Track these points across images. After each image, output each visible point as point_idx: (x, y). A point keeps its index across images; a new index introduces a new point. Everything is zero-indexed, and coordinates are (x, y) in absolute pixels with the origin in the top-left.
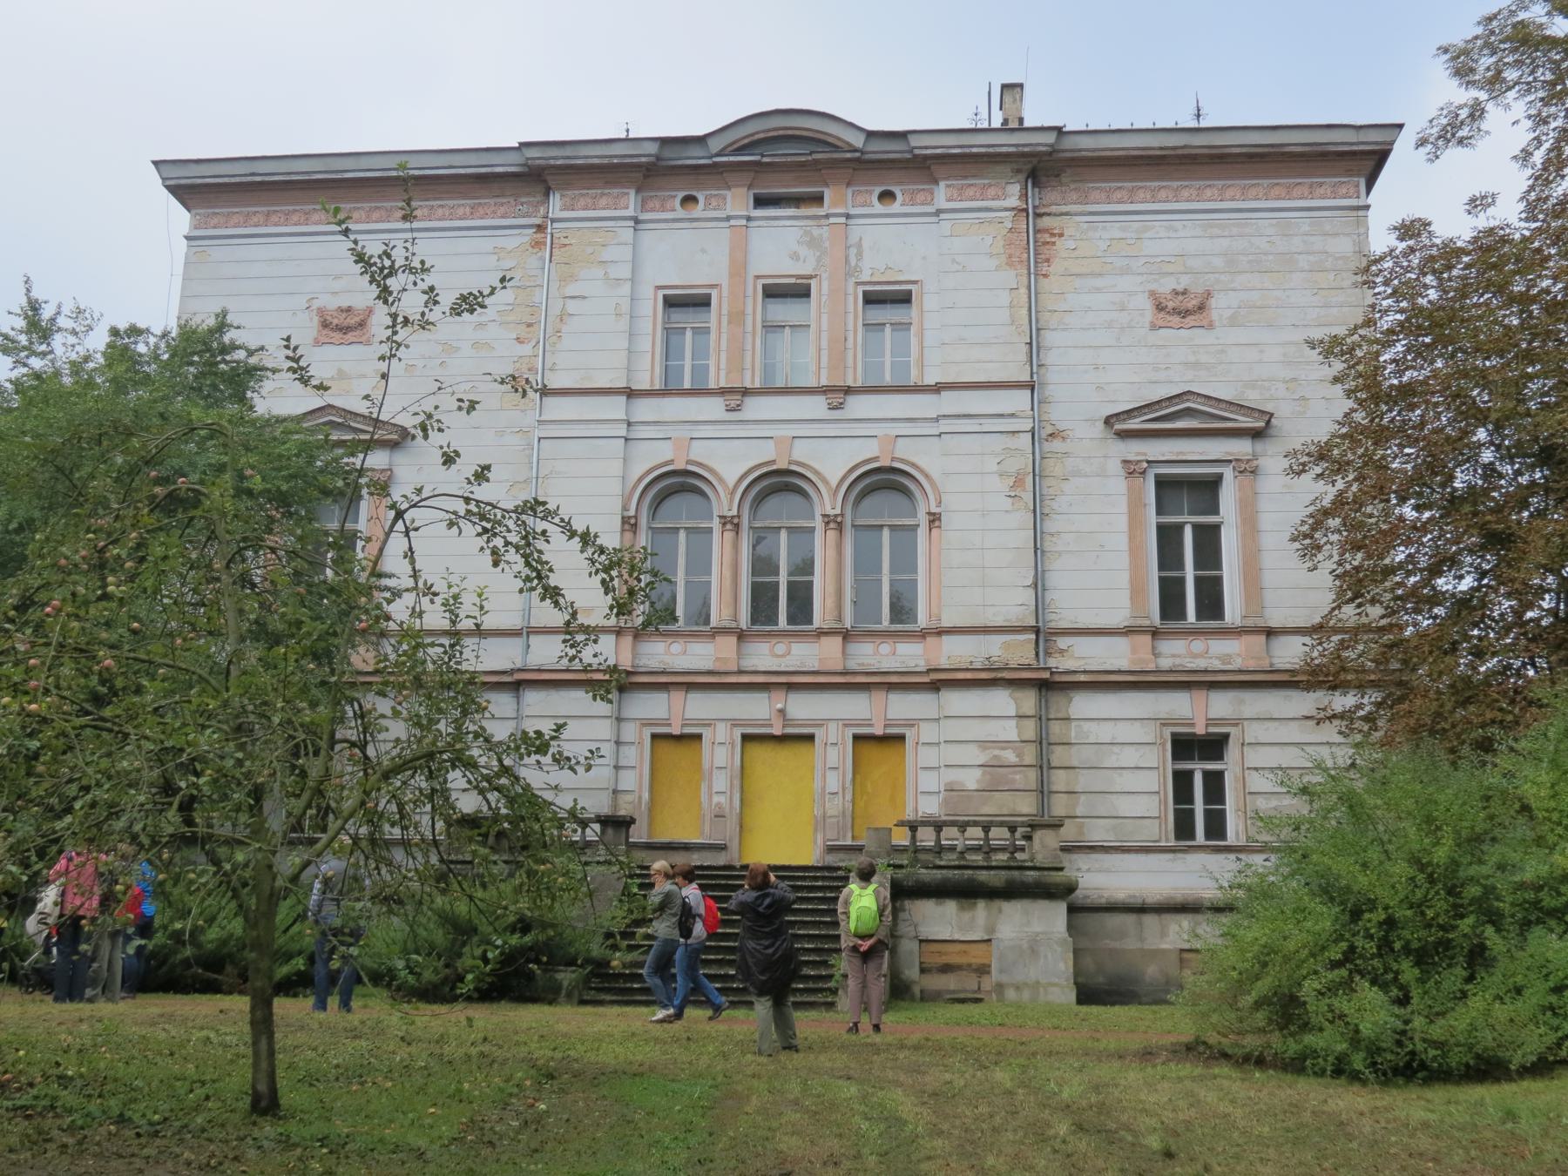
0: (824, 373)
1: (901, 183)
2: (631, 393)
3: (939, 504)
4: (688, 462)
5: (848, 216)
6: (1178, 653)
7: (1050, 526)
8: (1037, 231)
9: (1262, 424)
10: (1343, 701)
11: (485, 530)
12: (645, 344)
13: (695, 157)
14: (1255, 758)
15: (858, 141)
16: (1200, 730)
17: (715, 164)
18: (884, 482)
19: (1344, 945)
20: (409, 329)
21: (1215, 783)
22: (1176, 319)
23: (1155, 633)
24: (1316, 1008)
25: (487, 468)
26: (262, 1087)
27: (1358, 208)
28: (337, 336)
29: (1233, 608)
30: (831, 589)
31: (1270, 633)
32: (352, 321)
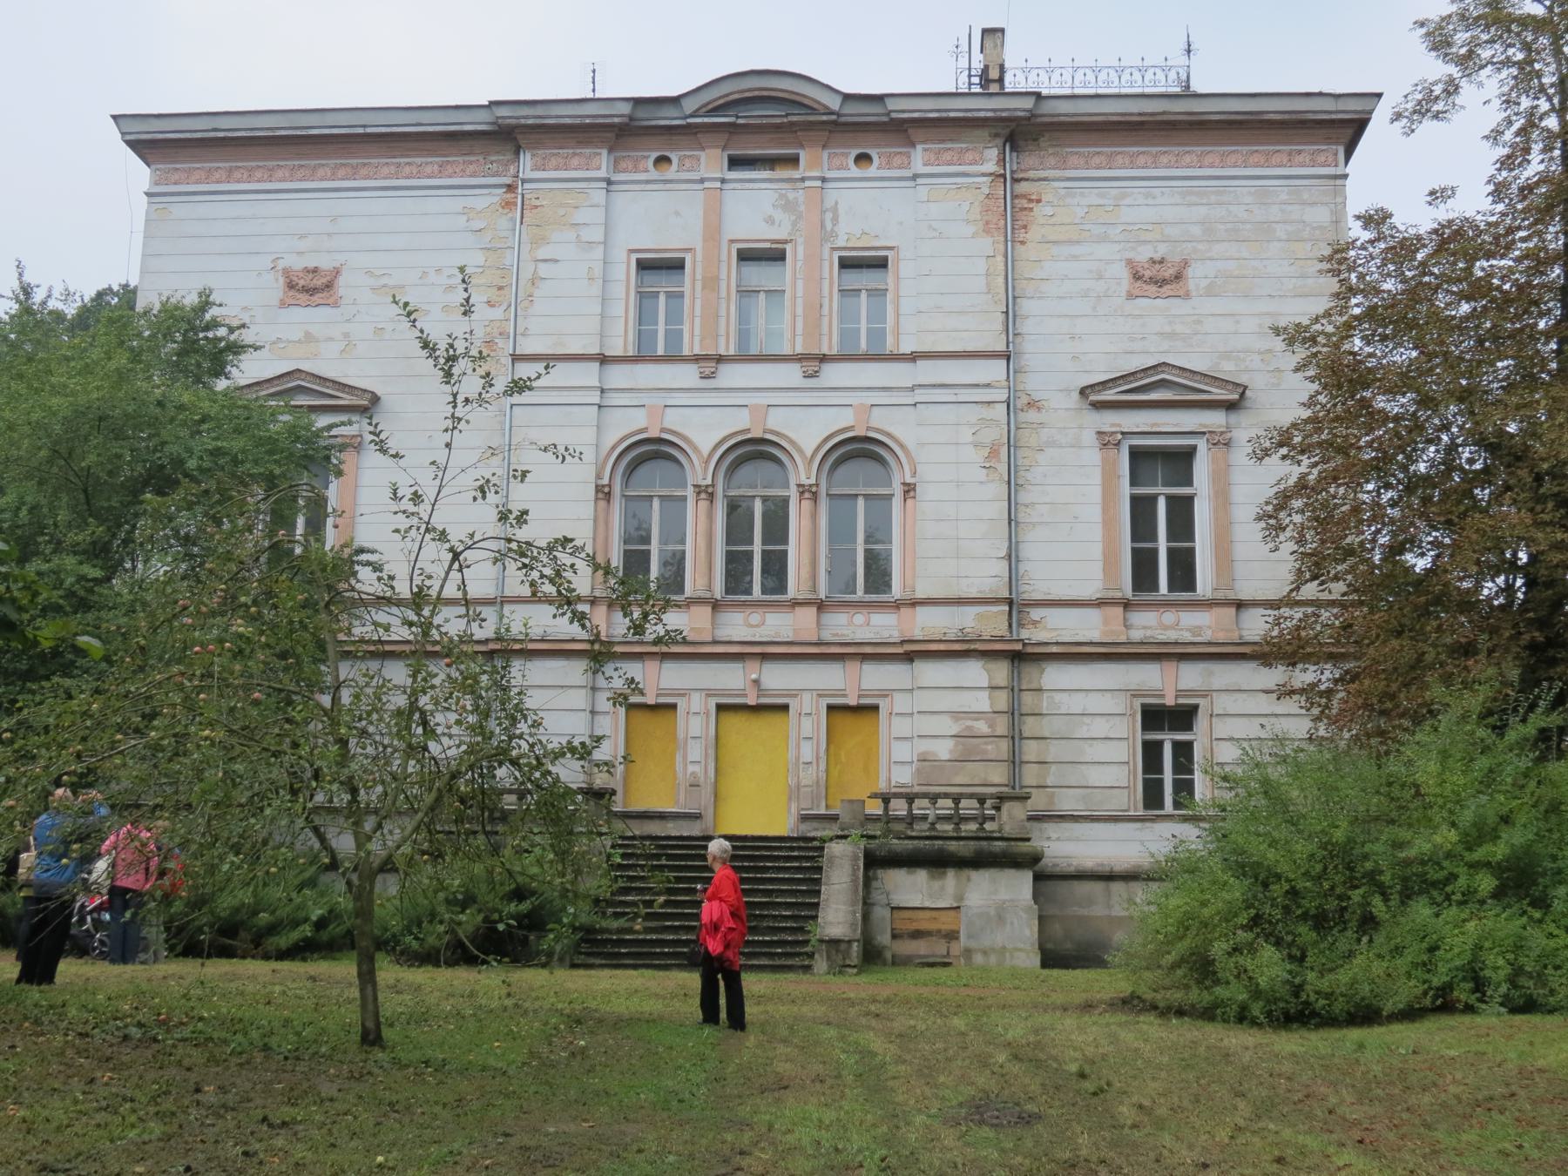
0: (799, 340)
1: (878, 146)
3: (914, 474)
4: (663, 430)
5: (824, 180)
6: (1149, 625)
7: (1024, 497)
8: (1014, 197)
9: (1236, 397)
10: (1305, 676)
11: (525, 566)
12: (618, 309)
13: (668, 117)
15: (834, 103)
16: (1170, 701)
17: (689, 126)
18: (859, 451)
19: (1253, 912)
20: (469, 407)
21: (1184, 751)
22: (1153, 288)
23: (1127, 605)
24: (1225, 966)
25: (526, 512)
26: (370, 1025)
27: (1336, 177)
28: (304, 297)
29: (1205, 579)
30: (806, 560)
31: (1240, 605)
32: (318, 282)
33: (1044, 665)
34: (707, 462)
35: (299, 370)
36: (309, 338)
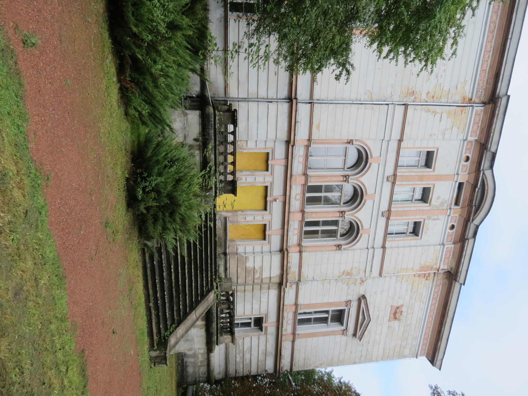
1: (456, 232)
2: (400, 141)
3: (344, 249)
6: (288, 316)
13: (485, 164)
14: (255, 340)
15: (476, 222)
33: (277, 290)
34: (357, 180)
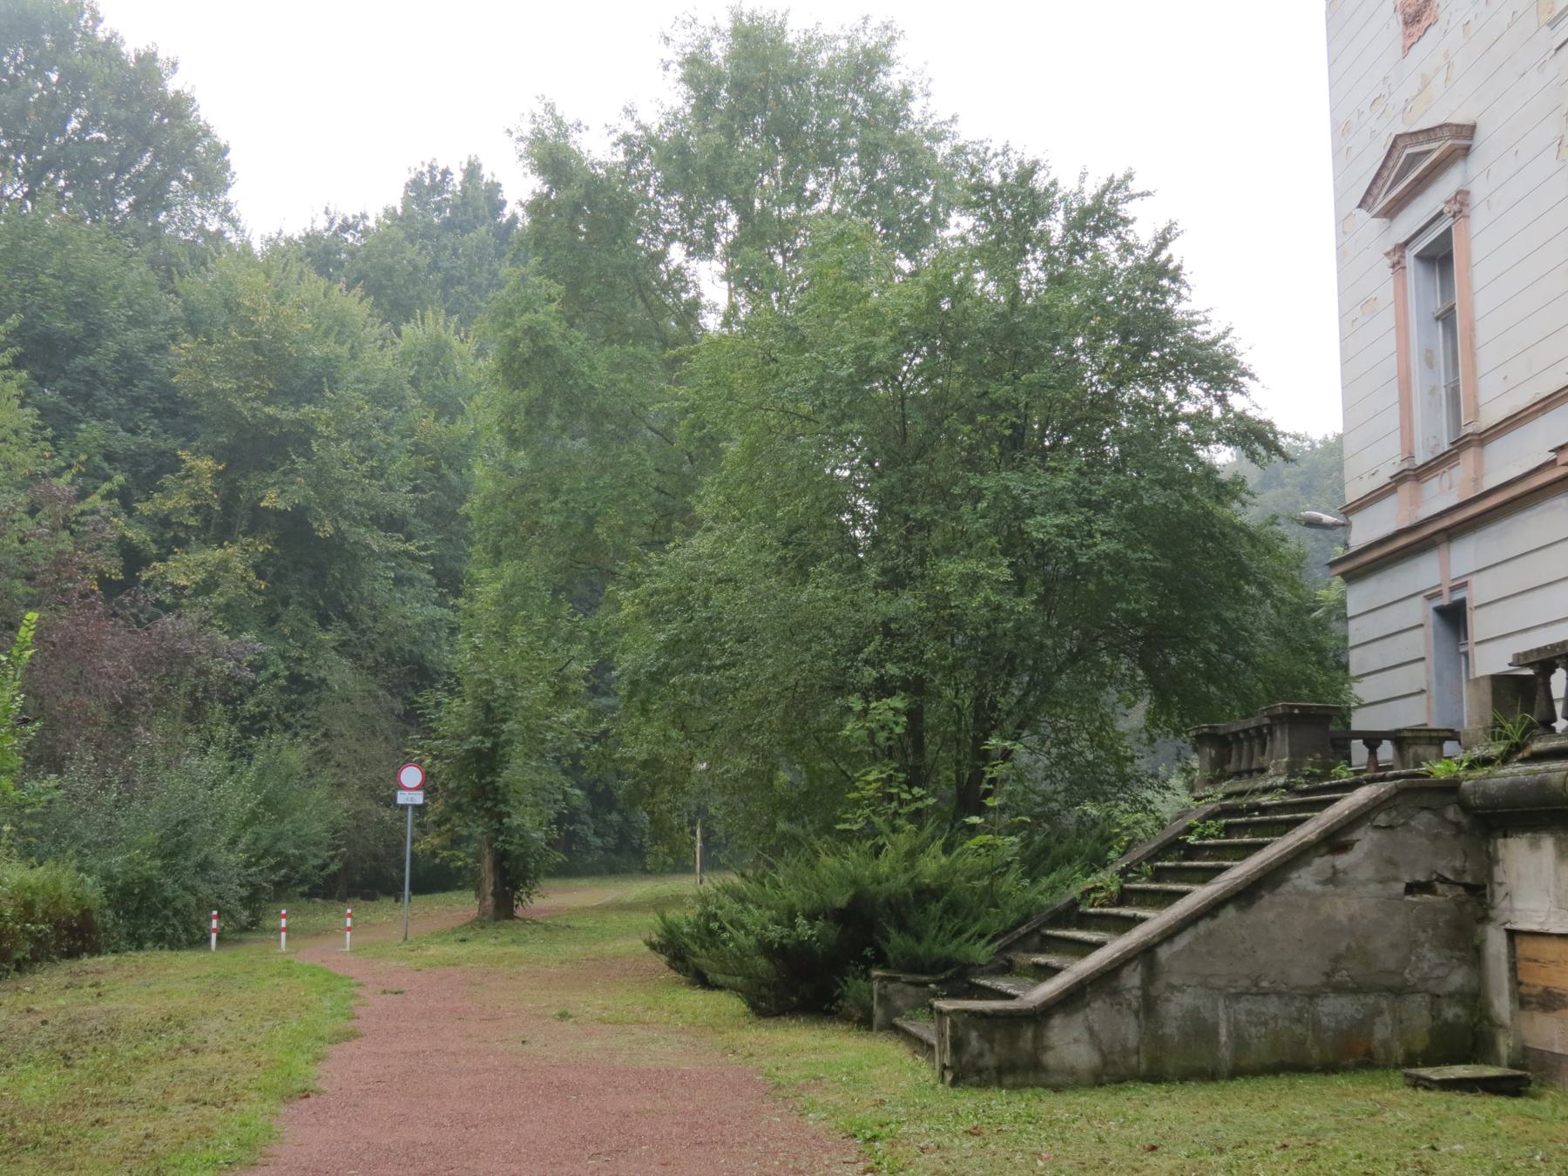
35: (1398, 137)
36: (1426, 84)
